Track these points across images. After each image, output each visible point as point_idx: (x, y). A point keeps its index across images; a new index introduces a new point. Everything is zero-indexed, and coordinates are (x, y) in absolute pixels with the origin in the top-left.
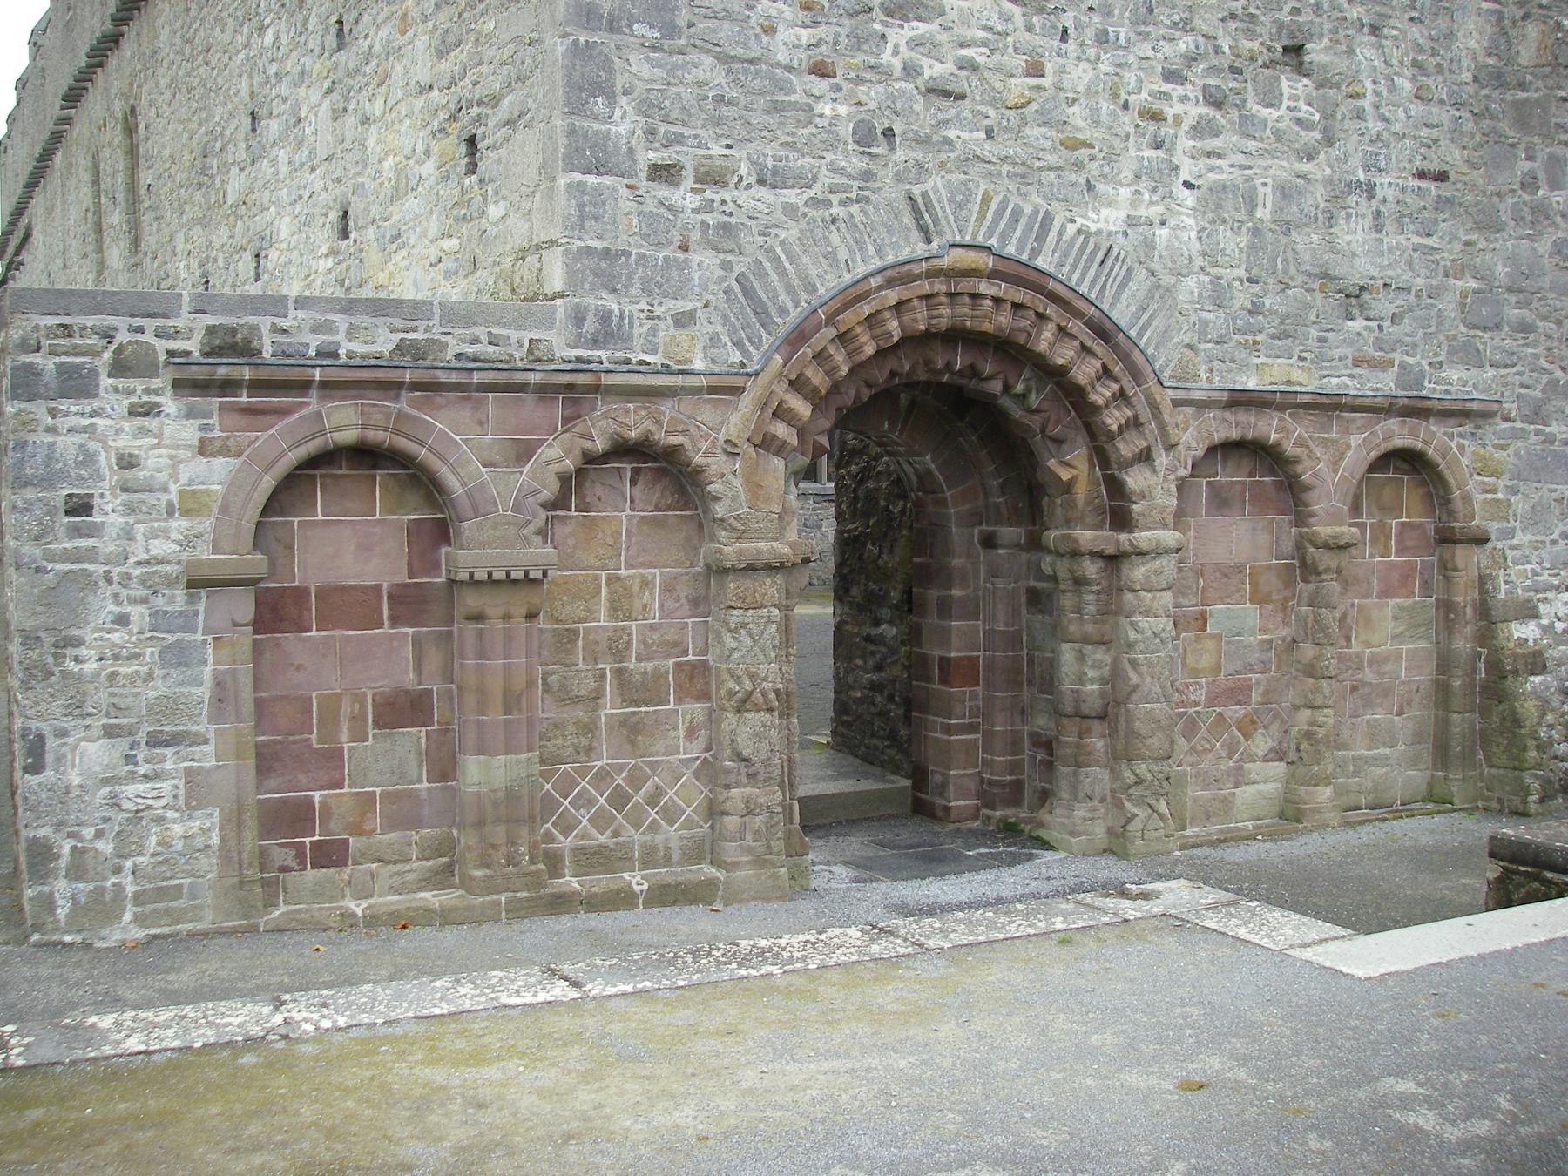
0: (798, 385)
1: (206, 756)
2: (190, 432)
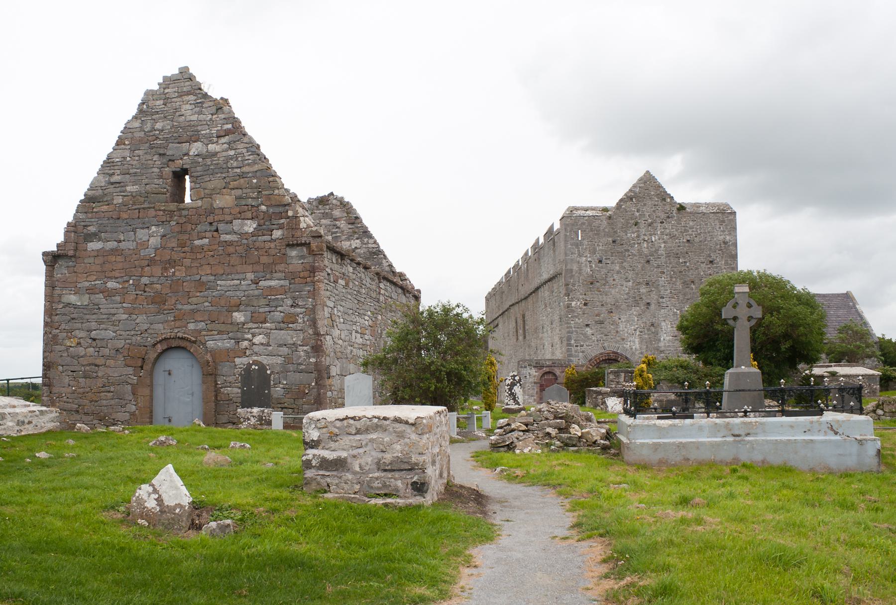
0: (591, 365)
1: (535, 398)
2: (534, 371)
